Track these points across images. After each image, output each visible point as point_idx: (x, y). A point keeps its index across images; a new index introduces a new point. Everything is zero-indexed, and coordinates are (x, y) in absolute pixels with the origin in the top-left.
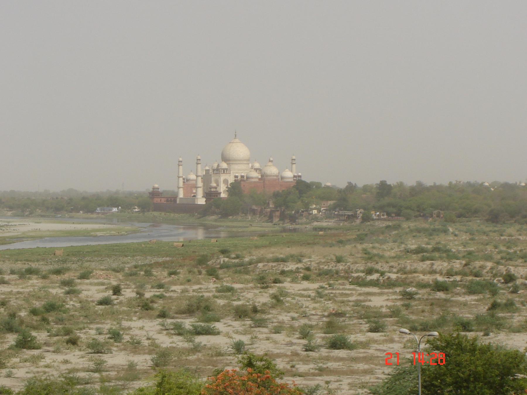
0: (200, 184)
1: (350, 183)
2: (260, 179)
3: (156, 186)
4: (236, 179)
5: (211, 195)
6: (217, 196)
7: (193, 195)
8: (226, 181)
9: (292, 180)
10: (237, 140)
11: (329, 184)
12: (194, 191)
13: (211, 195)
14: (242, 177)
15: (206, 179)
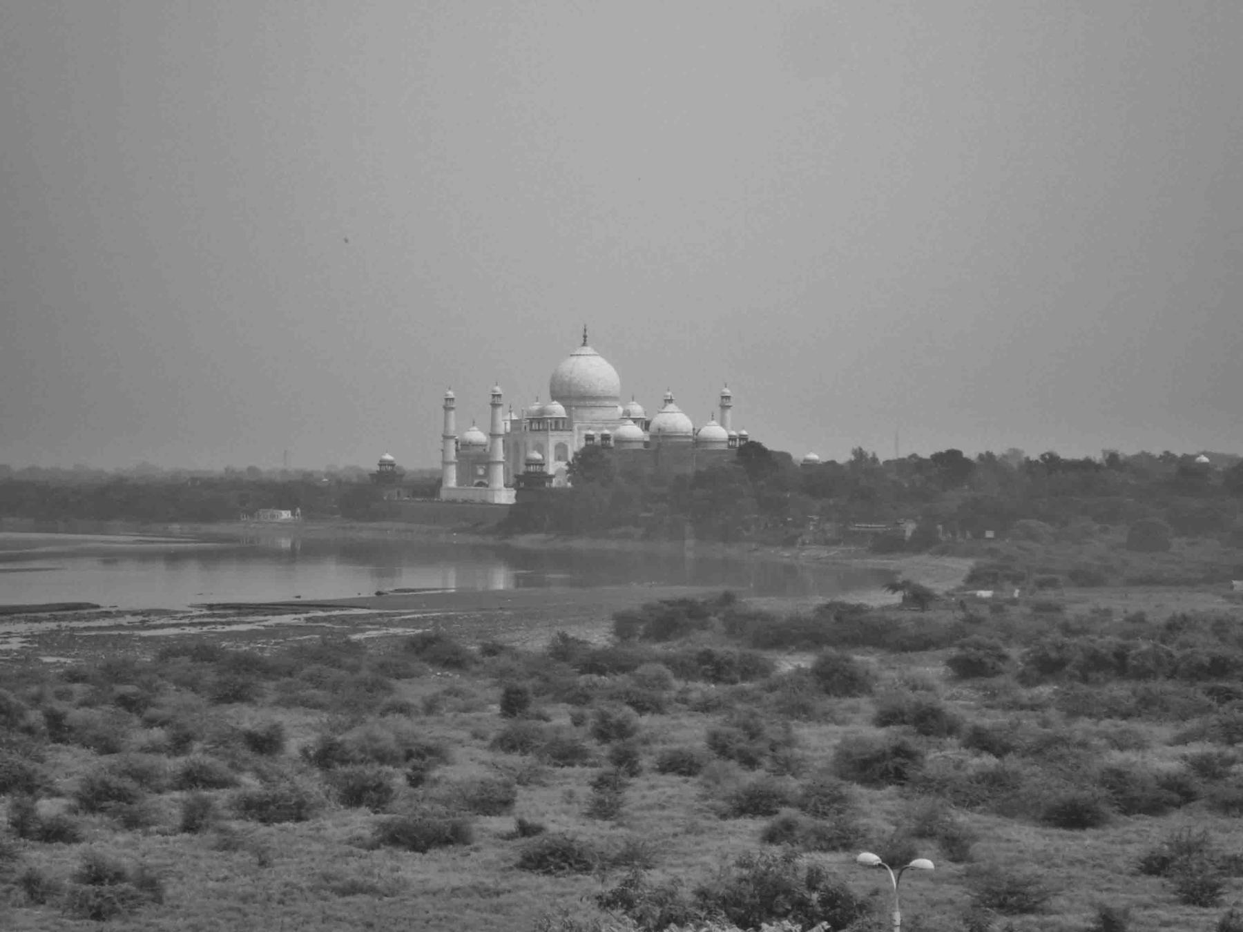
0: (500, 456)
1: (859, 454)
2: (646, 444)
3: (388, 457)
4: (590, 442)
5: (530, 481)
6: (544, 483)
7: (476, 481)
8: (561, 448)
9: (724, 447)
10: (588, 350)
11: (813, 456)
12: (481, 472)
13: (530, 481)
14: (605, 438)
15: (514, 445)
